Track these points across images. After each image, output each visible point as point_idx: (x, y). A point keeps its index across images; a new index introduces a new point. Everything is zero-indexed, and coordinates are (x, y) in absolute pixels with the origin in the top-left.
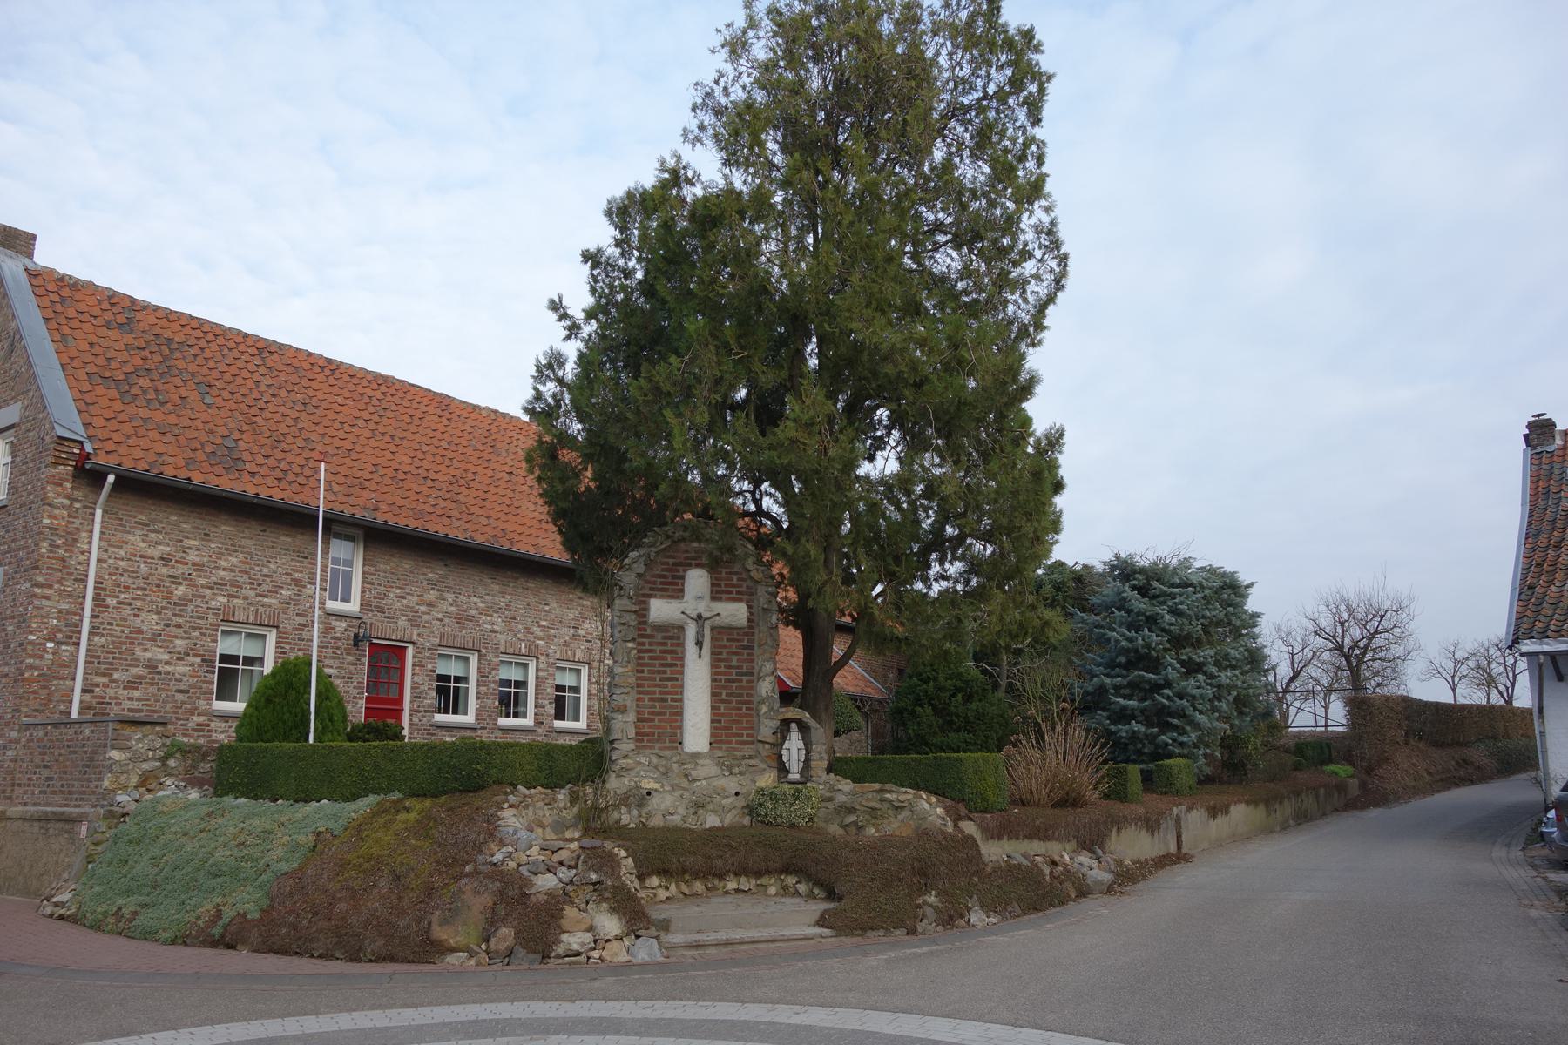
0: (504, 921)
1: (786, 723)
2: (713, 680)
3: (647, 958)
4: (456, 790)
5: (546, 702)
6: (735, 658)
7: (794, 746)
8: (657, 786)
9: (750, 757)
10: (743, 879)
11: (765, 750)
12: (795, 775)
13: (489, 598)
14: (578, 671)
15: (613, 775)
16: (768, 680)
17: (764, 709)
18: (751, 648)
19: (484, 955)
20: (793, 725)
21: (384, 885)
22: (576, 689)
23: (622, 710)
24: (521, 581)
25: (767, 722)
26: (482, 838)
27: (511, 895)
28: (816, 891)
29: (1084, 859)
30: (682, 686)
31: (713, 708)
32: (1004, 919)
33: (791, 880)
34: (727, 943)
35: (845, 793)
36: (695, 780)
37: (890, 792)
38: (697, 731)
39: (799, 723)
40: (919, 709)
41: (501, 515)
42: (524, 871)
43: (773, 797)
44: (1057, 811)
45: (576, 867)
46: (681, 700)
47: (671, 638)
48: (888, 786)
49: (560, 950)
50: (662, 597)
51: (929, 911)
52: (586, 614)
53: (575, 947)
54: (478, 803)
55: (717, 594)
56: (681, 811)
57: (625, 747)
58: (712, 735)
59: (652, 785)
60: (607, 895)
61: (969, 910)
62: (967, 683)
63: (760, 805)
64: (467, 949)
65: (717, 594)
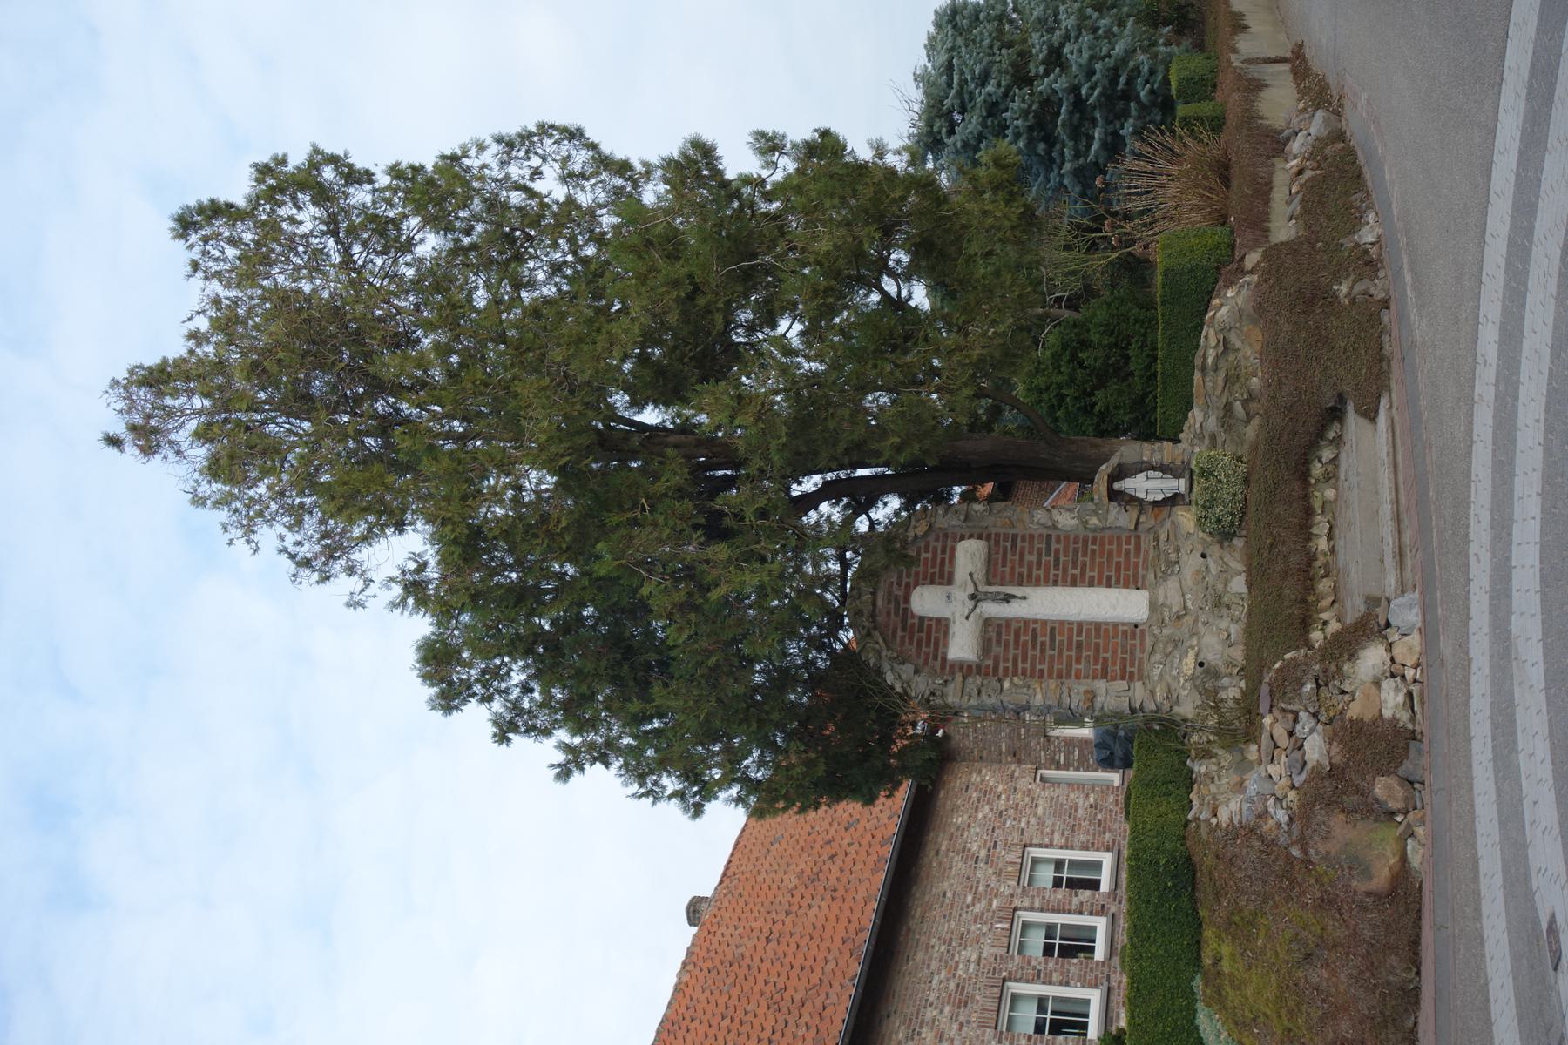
0: (1363, 793)
1: (1114, 495)
2: (1055, 583)
3: (1416, 610)
4: (1191, 896)
5: (1075, 901)
6: (1027, 558)
7: (1143, 485)
9: (1157, 539)
10: (1315, 530)
11: (1147, 521)
12: (1181, 485)
13: (934, 965)
14: (1035, 861)
15: (1176, 709)
16: (1056, 516)
17: (1094, 521)
18: (1015, 537)
19: (1411, 816)
20: (1117, 486)
21: (1317, 975)
22: (1059, 865)
23: (1091, 696)
24: (913, 923)
25: (1111, 518)
26: (1256, 843)
27: (1334, 790)
28: (1331, 435)
29: (1296, 146)
30: (1062, 623)
31: (1091, 585)
32: (1370, 207)
33: (1317, 470)
34: (1398, 519)
35: (1206, 419)
36: (1185, 608)
37: (1205, 357)
38: (1121, 605)
40: (1097, 408)
41: (823, 946)
42: (1299, 780)
43: (1208, 505)
44: (1235, 183)
45: (1296, 713)
46: (1080, 624)
47: (999, 634)
48: (1198, 361)
49: (1404, 716)
50: (946, 645)
51: (1358, 288)
52: (959, 847)
53: (1401, 698)
54: (1210, 860)
55: (944, 577)
57: (1139, 693)
58: (1126, 586)
59: (1190, 661)
60: (1333, 668)
61: (1358, 245)
62: (1065, 346)
63: (1219, 521)
64: (1403, 840)
65: (944, 577)
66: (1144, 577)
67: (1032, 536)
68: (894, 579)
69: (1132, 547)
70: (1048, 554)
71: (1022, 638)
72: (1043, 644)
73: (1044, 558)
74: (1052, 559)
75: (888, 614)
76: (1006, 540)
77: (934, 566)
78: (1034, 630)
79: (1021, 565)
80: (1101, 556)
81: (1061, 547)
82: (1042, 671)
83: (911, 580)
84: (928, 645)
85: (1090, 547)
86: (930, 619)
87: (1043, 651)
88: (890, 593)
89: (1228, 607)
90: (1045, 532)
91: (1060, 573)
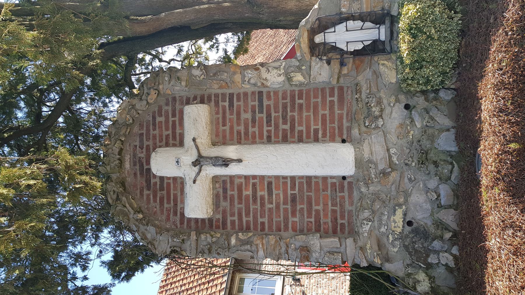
2: (269, 141)
6: (244, 116)
8: (399, 213)
17: (298, 78)
18: (231, 95)
20: (319, 39)
30: (277, 177)
31: (300, 140)
36: (391, 162)
39: (313, 32)
46: (293, 178)
47: (225, 190)
50: (183, 202)
55: (176, 140)
56: (433, 183)
58: (333, 140)
65: (176, 140)
66: (349, 129)
67: (246, 94)
68: (137, 143)
69: (335, 99)
71: (245, 193)
72: (262, 198)
73: (258, 115)
74: (264, 115)
75: (135, 174)
76: (224, 100)
77: (167, 129)
78: (254, 185)
80: (308, 110)
81: (271, 103)
82: (263, 224)
83: (151, 143)
84: (169, 202)
85: (298, 101)
86: (169, 178)
87: (263, 205)
88: (135, 155)
89: (436, 164)
90: (257, 89)
91: (272, 128)
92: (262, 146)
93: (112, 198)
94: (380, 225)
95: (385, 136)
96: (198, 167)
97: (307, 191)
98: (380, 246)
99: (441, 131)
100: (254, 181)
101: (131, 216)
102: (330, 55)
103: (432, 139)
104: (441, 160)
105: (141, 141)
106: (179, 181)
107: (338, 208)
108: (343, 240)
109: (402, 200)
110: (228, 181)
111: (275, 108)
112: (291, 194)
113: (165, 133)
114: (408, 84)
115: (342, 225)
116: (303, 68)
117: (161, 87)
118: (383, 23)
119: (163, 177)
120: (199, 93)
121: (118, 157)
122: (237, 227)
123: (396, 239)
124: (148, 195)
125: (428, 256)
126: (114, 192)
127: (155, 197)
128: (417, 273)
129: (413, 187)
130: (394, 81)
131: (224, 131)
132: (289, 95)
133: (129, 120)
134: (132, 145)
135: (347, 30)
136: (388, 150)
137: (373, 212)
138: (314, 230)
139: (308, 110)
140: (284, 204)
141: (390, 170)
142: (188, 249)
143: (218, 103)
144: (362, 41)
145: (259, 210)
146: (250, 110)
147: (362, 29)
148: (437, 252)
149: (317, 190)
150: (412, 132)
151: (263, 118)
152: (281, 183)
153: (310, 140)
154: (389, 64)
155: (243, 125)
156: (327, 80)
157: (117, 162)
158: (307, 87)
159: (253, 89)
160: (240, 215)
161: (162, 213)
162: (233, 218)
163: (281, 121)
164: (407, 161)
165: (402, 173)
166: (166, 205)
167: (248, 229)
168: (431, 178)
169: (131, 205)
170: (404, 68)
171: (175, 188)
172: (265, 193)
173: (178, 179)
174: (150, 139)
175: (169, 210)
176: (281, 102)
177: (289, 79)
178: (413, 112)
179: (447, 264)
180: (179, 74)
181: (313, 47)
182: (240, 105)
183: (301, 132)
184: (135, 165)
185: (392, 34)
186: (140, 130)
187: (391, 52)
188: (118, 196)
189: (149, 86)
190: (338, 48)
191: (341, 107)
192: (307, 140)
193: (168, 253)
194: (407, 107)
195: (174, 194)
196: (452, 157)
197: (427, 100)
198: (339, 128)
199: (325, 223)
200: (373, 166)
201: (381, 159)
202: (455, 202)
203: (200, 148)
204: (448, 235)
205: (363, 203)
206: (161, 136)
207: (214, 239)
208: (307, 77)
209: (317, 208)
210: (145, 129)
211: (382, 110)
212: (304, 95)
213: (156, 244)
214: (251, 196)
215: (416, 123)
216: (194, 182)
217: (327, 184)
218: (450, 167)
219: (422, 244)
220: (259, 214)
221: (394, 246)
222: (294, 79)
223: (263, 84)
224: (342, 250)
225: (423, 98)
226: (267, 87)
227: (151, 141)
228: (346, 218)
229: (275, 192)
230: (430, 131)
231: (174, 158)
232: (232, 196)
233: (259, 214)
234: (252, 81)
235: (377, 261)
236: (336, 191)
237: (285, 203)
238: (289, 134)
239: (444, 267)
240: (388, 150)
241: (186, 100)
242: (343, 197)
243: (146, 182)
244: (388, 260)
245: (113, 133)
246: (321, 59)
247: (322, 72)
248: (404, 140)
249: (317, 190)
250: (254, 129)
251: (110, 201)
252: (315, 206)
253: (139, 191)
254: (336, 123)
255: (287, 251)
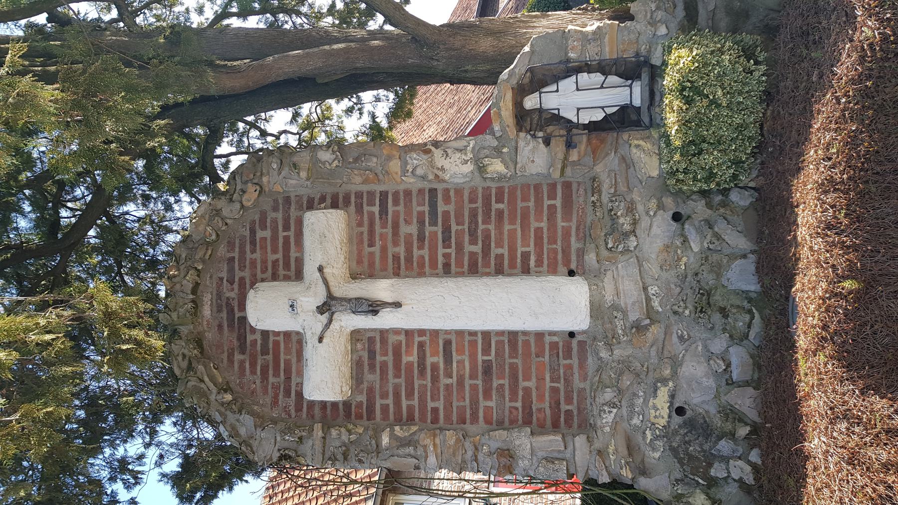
2: (447, 271)
6: (404, 229)
8: (663, 393)
12: (636, 94)
17: (497, 167)
18: (384, 195)
20: (530, 102)
30: (460, 333)
31: (499, 271)
39: (521, 91)
46: (486, 335)
47: (372, 354)
50: (300, 374)
55: (290, 270)
56: (719, 344)
65: (290, 270)
66: (581, 253)
67: (408, 193)
68: (224, 275)
69: (558, 202)
70: (434, 223)
71: (405, 359)
72: (435, 367)
73: (428, 229)
74: (439, 229)
75: (220, 327)
76: (371, 203)
77: (275, 251)
78: (421, 345)
79: (396, 243)
80: (512, 221)
81: (451, 208)
82: (435, 410)
83: (247, 274)
84: (276, 374)
85: (495, 206)
86: (277, 334)
87: (435, 379)
89: (724, 312)
90: (427, 186)
91: (452, 251)
92: (435, 281)
93: (179, 367)
94: (631, 414)
95: (641, 266)
96: (327, 315)
97: (511, 357)
98: (631, 448)
99: (732, 257)
100: (421, 339)
101: (213, 397)
102: (550, 129)
103: (718, 270)
104: (732, 306)
105: (231, 270)
106: (294, 338)
107: (561, 386)
108: (569, 438)
109: (667, 372)
110: (378, 339)
111: (456, 217)
112: (484, 361)
113: (271, 257)
114: (678, 181)
115: (568, 413)
116: (505, 150)
117: (265, 179)
118: (639, 77)
119: (268, 331)
120: (329, 190)
121: (191, 297)
122: (392, 417)
123: (657, 438)
124: (242, 363)
125: (710, 465)
126: (184, 356)
127: (253, 365)
128: (691, 494)
129: (686, 351)
130: (655, 173)
131: (371, 254)
132: (480, 195)
133: (211, 235)
134: (215, 276)
135: (578, 89)
136: (645, 289)
137: (620, 392)
138: (520, 422)
139: (512, 221)
140: (471, 378)
141: (648, 321)
142: (309, 453)
143: (362, 207)
144: (602, 108)
145: (429, 388)
146: (415, 220)
147: (602, 87)
148: (725, 459)
149: (527, 355)
150: (685, 259)
151: (436, 233)
152: (466, 344)
153: (515, 271)
154: (647, 146)
155: (403, 244)
156: (545, 171)
157: (190, 305)
158: (511, 183)
159: (420, 185)
160: (397, 395)
161: (265, 392)
162: (385, 402)
163: (467, 238)
164: (676, 308)
165: (668, 328)
166: (272, 379)
167: (411, 419)
168: (715, 336)
169: (213, 379)
170: (672, 152)
171: (288, 351)
172: (440, 360)
173: (293, 335)
174: (245, 267)
175: (276, 388)
176: (467, 206)
177: (481, 169)
178: (686, 226)
179: (741, 478)
180: (295, 159)
181: (522, 116)
182: (398, 212)
183: (500, 257)
184: (219, 310)
185: (653, 95)
186: (228, 252)
187: (651, 125)
188: (190, 363)
189: (245, 178)
190: (563, 117)
191: (567, 216)
192: (509, 271)
193: (275, 460)
194: (677, 217)
195: (285, 360)
196: (750, 300)
197: (709, 205)
198: (563, 251)
199: (539, 410)
200: (619, 315)
201: (633, 304)
202: (756, 376)
203: (331, 284)
204: (743, 431)
205: (604, 376)
206: (264, 262)
207: (353, 437)
208: (512, 166)
209: (527, 384)
210: (237, 250)
211: (635, 223)
212: (506, 195)
213: (255, 444)
214: (416, 365)
215: (692, 244)
216: (320, 340)
217: (544, 346)
218: (747, 317)
219: (701, 445)
220: (429, 394)
221: (654, 450)
222: (490, 169)
223: (437, 176)
224: (568, 455)
225: (703, 202)
226: (444, 181)
227: (247, 270)
228: (575, 401)
229: (455, 357)
230: (715, 258)
231: (286, 300)
232: (384, 365)
233: (429, 394)
234: (419, 172)
235: (626, 474)
236: (558, 356)
237: (473, 376)
238: (480, 260)
239: (736, 485)
240: (645, 289)
241: (308, 202)
242: (570, 367)
243: (239, 339)
244: (643, 471)
245: (184, 256)
246: (534, 136)
247: (536, 158)
248: (673, 272)
249: (527, 355)
250: (421, 252)
251: (177, 372)
252: (524, 380)
253: (226, 354)
254: (559, 243)
255: (476, 456)
